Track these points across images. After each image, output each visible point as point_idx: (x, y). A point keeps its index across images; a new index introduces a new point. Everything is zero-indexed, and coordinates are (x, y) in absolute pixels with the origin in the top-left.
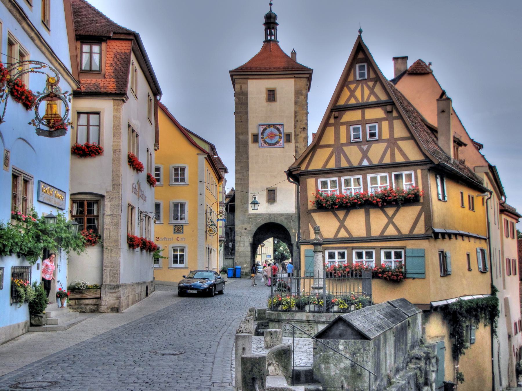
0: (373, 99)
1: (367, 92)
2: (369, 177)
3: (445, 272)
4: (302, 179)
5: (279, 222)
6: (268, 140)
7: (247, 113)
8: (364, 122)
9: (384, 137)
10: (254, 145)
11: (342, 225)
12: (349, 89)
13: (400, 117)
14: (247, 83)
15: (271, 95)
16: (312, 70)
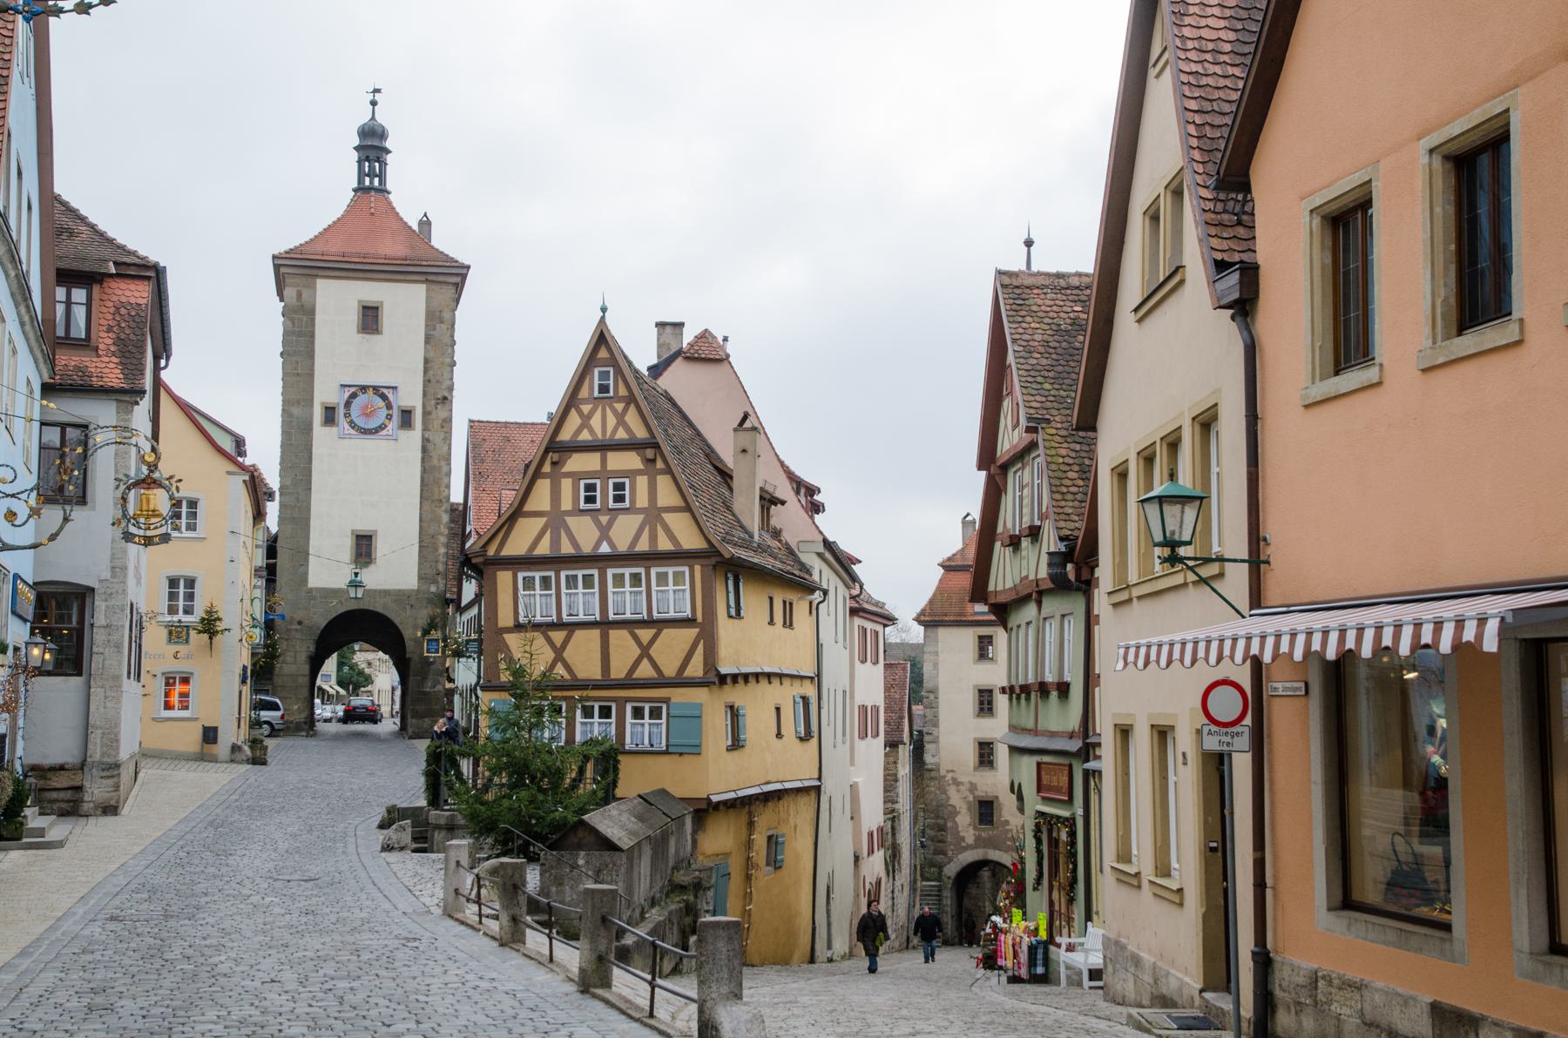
0: (621, 435)
1: (611, 421)
2: (610, 572)
3: (736, 744)
4: (488, 571)
5: (379, 610)
6: (360, 422)
7: (311, 355)
8: (604, 474)
9: (638, 505)
10: (328, 429)
11: (559, 656)
13: (668, 470)
14: (314, 288)
15: (370, 318)
16: (468, 267)
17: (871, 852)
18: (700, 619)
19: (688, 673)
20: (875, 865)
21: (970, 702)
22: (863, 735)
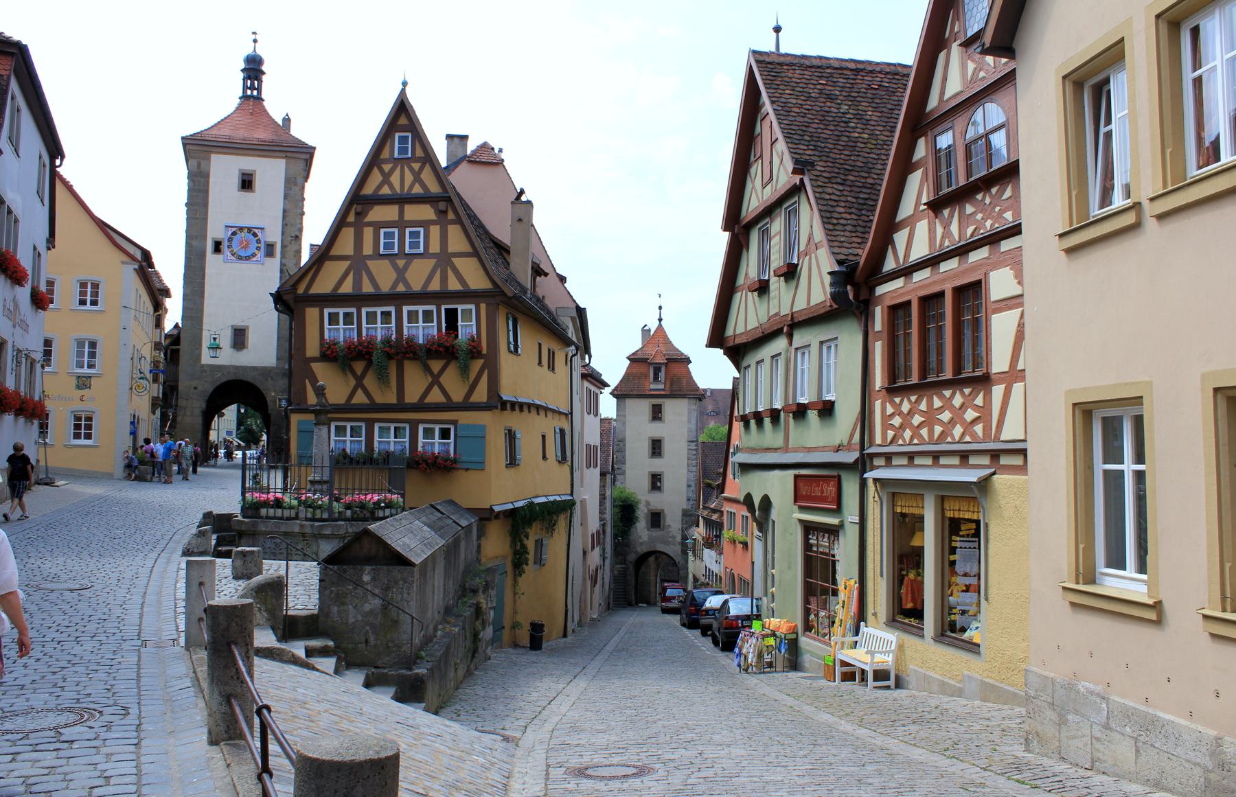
0: (417, 189)
1: (409, 178)
2: (405, 309)
3: (512, 462)
5: (250, 380)
7: (206, 205)
12: (381, 171)
13: (459, 221)
14: (209, 159)
15: (247, 183)
16: (314, 148)
17: (593, 548)
18: (484, 352)
19: (475, 398)
20: (595, 557)
21: (646, 448)
22: (588, 466)
